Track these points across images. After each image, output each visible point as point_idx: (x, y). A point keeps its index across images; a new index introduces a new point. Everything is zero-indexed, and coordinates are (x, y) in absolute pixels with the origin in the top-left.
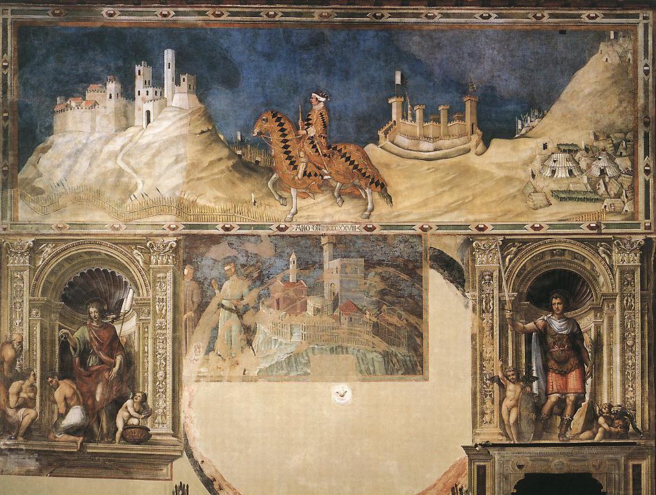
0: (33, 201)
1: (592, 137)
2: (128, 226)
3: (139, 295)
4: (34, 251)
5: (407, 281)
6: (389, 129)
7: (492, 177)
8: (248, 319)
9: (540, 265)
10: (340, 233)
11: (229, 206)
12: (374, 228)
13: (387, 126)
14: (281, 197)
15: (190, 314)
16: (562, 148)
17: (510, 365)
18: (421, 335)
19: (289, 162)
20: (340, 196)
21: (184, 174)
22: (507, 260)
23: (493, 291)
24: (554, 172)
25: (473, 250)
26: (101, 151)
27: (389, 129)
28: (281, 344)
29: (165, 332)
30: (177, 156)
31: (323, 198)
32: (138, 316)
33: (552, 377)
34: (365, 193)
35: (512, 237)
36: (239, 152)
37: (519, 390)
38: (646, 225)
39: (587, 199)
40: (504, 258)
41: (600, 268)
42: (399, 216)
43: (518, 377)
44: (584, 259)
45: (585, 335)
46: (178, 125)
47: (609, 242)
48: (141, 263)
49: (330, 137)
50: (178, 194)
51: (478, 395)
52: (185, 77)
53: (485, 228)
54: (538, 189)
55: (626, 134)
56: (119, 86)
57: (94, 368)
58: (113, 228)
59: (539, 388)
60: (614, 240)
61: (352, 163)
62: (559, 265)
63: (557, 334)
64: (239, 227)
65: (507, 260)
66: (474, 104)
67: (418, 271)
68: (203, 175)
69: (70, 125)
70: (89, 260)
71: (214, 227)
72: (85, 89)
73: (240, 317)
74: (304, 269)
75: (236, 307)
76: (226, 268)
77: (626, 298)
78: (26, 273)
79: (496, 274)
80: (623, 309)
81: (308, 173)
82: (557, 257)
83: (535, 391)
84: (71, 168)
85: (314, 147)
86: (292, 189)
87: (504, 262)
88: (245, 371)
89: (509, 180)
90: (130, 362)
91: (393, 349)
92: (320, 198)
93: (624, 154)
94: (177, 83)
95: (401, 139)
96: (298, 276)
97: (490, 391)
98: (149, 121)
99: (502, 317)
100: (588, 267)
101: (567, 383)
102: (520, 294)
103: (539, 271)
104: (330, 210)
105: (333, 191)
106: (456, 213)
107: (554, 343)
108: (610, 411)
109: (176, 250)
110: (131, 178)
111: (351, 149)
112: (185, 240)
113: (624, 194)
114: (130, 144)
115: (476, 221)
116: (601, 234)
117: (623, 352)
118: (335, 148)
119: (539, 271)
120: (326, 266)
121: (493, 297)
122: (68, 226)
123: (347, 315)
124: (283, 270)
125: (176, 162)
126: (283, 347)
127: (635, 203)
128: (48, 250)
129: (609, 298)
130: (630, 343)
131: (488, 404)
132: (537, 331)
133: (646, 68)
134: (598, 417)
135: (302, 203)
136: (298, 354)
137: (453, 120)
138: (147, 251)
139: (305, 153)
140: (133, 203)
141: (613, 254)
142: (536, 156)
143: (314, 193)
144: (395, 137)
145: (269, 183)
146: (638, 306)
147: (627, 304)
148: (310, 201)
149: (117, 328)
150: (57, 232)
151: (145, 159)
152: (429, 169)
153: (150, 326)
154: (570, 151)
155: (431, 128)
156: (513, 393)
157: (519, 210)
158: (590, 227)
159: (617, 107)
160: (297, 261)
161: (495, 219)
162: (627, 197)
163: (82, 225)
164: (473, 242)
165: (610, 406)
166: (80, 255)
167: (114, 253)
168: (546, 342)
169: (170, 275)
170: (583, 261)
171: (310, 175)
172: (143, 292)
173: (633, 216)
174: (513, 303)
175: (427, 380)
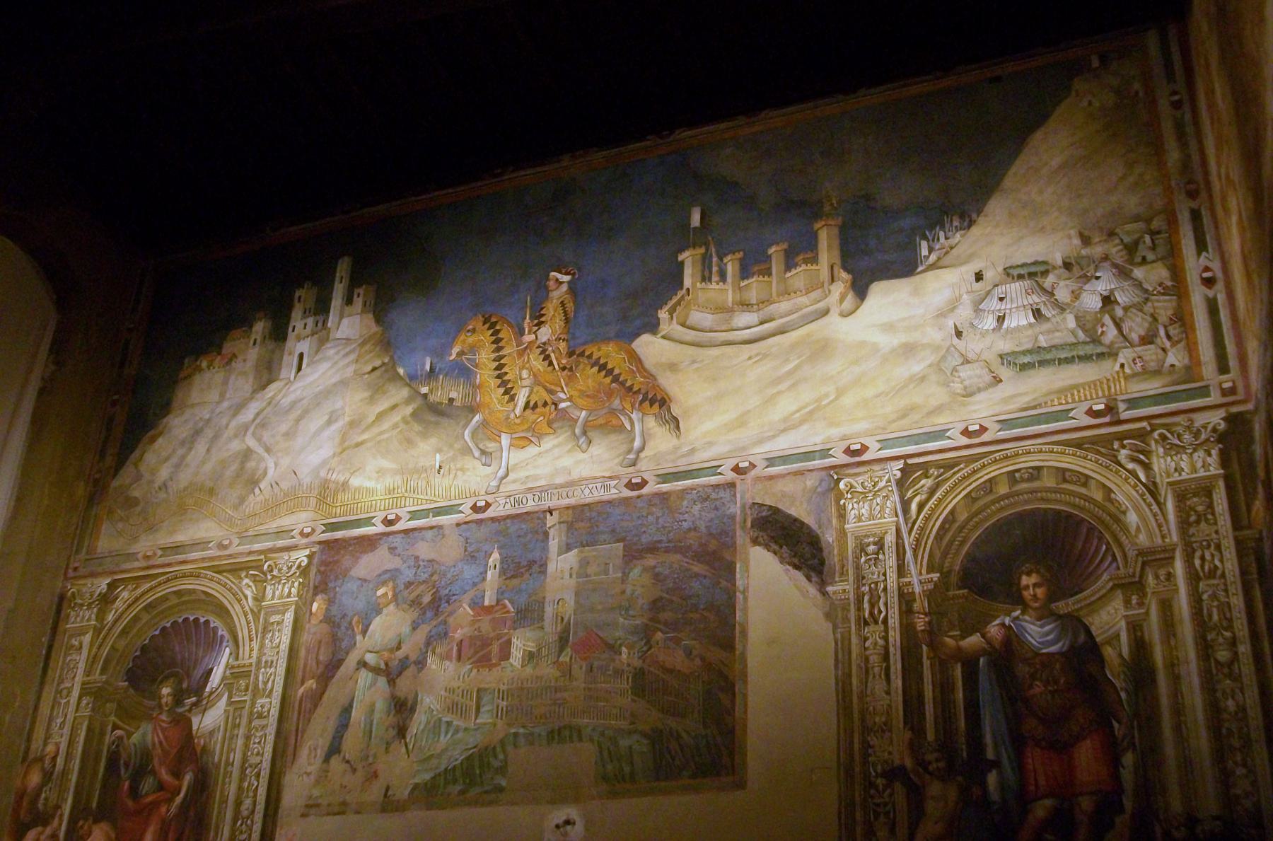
0: (121, 519)
1: (1077, 241)
2: (242, 537)
3: (237, 659)
4: (106, 600)
5: (705, 577)
6: (679, 303)
7: (875, 348)
8: (404, 685)
9: (986, 506)
10: (583, 502)
11: (398, 479)
12: (644, 483)
13: (675, 300)
14: (483, 452)
15: (311, 684)
16: (1015, 272)
17: (931, 736)
18: (729, 688)
19: (502, 390)
20: (584, 433)
21: (337, 440)
22: (914, 506)
23: (885, 575)
24: (1001, 319)
25: (840, 495)
26: (227, 425)
27: (679, 303)
28: (457, 731)
29: (264, 722)
30: (332, 413)
31: (555, 442)
32: (230, 697)
33: (1035, 759)
34: (631, 419)
35: (922, 460)
36: (424, 390)
37: (953, 794)
38: (1227, 385)
39: (1080, 358)
41: (1125, 494)
42: (693, 451)
44: (1085, 480)
45: (1108, 652)
46: (341, 364)
47: (1142, 435)
48: (250, 599)
49: (574, 338)
50: (323, 474)
51: (859, 815)
52: (361, 291)
53: (864, 449)
54: (971, 356)
55: (1148, 221)
56: (269, 324)
57: (150, 799)
58: (221, 546)
59: (1002, 787)
60: (1153, 430)
61: (610, 372)
62: (1026, 502)
63: (1038, 654)
64: (408, 516)
65: (914, 506)
66: (836, 231)
67: (727, 556)
68: (365, 437)
69: (195, 396)
70: (178, 605)
71: (368, 521)
72: (224, 339)
73: (392, 682)
74: (513, 577)
75: (387, 665)
76: (380, 592)
77: (1198, 554)
78: (87, 639)
79: (890, 539)
80: (1194, 578)
81: (532, 404)
82: (1025, 486)
84: (183, 457)
85: (547, 358)
86: (503, 436)
87: (906, 510)
88: (387, 790)
89: (909, 350)
90: (203, 786)
91: (672, 723)
92: (549, 442)
93: (1150, 257)
94: (349, 301)
95: (697, 317)
96: (501, 592)
97: (886, 805)
98: (299, 369)
99: (907, 628)
100: (1098, 496)
102: (945, 575)
104: (567, 461)
105: (573, 427)
106: (805, 427)
107: (1033, 677)
109: (304, 571)
110: (262, 459)
111: (611, 353)
112: (322, 551)
113: (1162, 332)
114: (269, 409)
115: (843, 439)
116: (1120, 422)
118: (582, 354)
119: (986, 519)
120: (551, 567)
121: (885, 589)
122: (160, 552)
123: (585, 659)
124: (475, 584)
125: (329, 422)
126: (460, 735)
127: (1192, 349)
128: (125, 594)
129: (1157, 558)
130: (1223, 655)
132: (990, 654)
133: (1176, 98)
135: (517, 456)
136: (486, 749)
137: (795, 266)
138: (259, 581)
139: (530, 370)
140: (255, 501)
141: (1154, 460)
142: (961, 296)
143: (540, 436)
144: (687, 316)
145: (467, 433)
146: (1230, 565)
147: (1202, 566)
148: (532, 450)
149: (195, 721)
150: (143, 564)
151: (284, 428)
152: (750, 358)
153: (245, 712)
154: (1031, 275)
155: (754, 287)
157: (934, 402)
158: (1091, 413)
159: (1123, 178)
160: (502, 562)
161: (884, 429)
162: (1169, 337)
163: (177, 548)
164: (839, 480)
165: (1192, 821)
166: (164, 599)
167: (215, 590)
169: (289, 617)
170: (1085, 485)
171: (536, 406)
172: (244, 650)
173: (1191, 371)
174: (930, 595)
175: (741, 785)
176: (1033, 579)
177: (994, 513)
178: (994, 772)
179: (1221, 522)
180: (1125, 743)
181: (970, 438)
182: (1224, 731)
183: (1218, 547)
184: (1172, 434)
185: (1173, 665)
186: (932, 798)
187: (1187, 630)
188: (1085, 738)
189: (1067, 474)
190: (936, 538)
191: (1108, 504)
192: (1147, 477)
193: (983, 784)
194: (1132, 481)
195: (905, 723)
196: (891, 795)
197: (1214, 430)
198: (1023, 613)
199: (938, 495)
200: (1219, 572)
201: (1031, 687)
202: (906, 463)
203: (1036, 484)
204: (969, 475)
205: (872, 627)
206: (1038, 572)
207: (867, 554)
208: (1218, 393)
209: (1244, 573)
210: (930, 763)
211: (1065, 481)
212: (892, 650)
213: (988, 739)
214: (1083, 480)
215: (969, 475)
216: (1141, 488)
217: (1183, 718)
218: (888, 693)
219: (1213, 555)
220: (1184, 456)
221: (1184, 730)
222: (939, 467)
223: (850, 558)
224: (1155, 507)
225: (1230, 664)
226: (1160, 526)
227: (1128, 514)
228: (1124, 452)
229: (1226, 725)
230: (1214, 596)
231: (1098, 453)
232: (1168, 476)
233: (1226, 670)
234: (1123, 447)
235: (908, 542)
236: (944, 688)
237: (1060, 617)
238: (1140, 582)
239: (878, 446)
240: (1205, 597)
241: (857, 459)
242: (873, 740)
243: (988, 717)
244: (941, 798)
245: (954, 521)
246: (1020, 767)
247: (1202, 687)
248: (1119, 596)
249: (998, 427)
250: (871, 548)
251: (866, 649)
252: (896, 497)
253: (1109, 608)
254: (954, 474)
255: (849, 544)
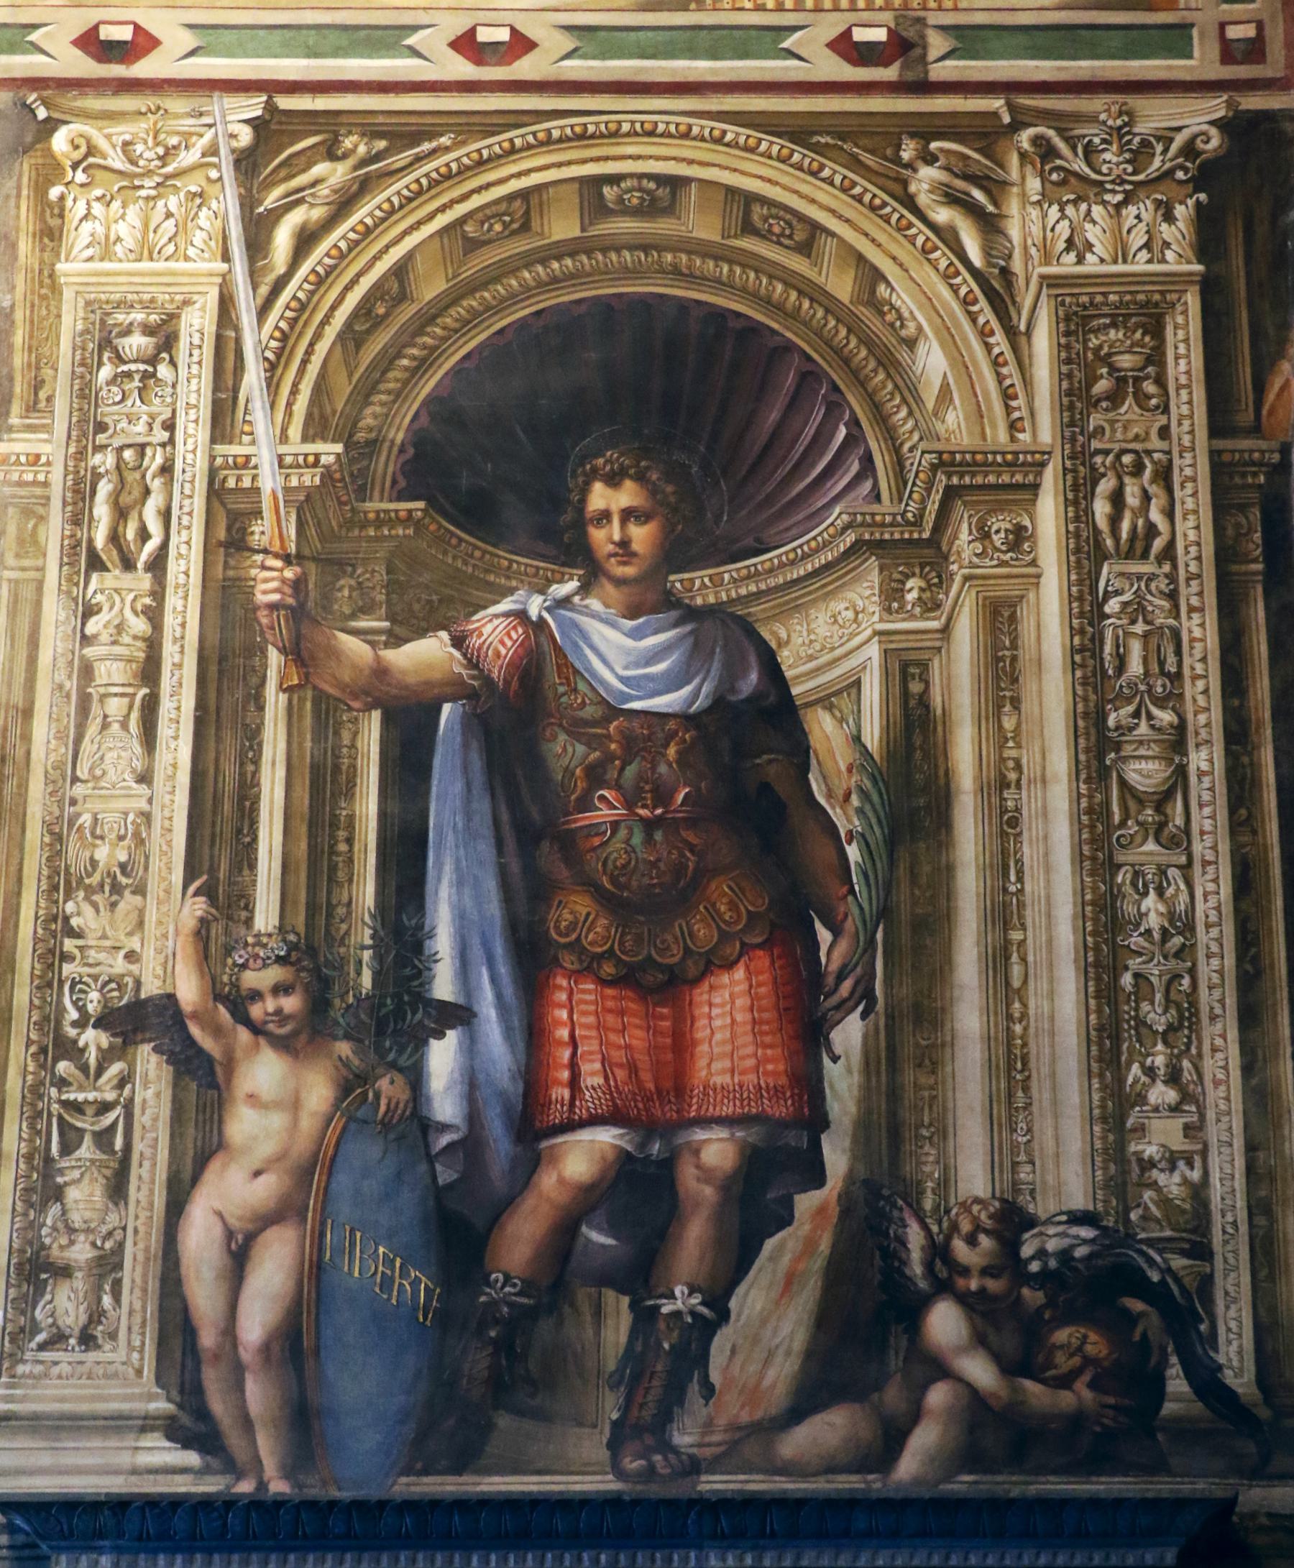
17: (265, 916)
22: (283, 238)
23: (170, 426)
25: (51, 171)
33: (576, 1009)
37: (318, 1092)
38: (1234, 32)
40: (257, 233)
41: (920, 292)
43: (318, 1005)
44: (809, 237)
45: (824, 729)
47: (987, 135)
53: (143, 43)
59: (472, 1083)
60: (1016, 126)
63: (614, 712)
65: (283, 238)
77: (1106, 486)
79: (198, 323)
80: (1086, 552)
83: (445, 1104)
87: (257, 245)
97: (105, 1107)
99: (225, 596)
100: (842, 286)
101: (681, 1044)
102: (361, 451)
103: (513, 299)
108: (1008, 1260)
116: (925, 87)
117: (1098, 852)
121: (166, 470)
129: (985, 483)
130: (1145, 772)
131: (84, 1194)
132: (471, 695)
134: (911, 1312)
141: (1013, 207)
146: (1193, 528)
147: (1115, 521)
156: (277, 1120)
158: (844, 46)
164: (51, 125)
165: (1012, 1220)
168: (535, 761)
170: (805, 249)
174: (306, 505)
176: (627, 496)
177: (527, 292)
178: (452, 1036)
179: (1178, 407)
180: (846, 986)
181: (479, 62)
182: (1127, 980)
183: (1164, 475)
184: (1071, 142)
185: (1003, 784)
186: (252, 1098)
187: (1051, 693)
188: (730, 966)
189: (758, 211)
190: (341, 337)
191: (865, 312)
192: (987, 252)
193: (416, 1078)
194: (943, 257)
195: (191, 872)
196: (122, 1082)
197: (1189, 150)
198: (585, 589)
199: (363, 213)
200: (1158, 544)
201: (585, 804)
202: (270, 107)
203: (662, 227)
204: (464, 171)
205: (114, 578)
206: (640, 478)
207: (120, 359)
208: (1214, 51)
209: (1226, 555)
210: (256, 995)
211: (748, 228)
212: (169, 651)
213: (443, 943)
214: (800, 236)
215: (464, 171)
216: (968, 284)
217: (1016, 936)
218: (145, 778)
219: (1146, 497)
220: (1097, 211)
221: (1016, 970)
222: (373, 133)
223: (64, 365)
224: (999, 340)
225: (1162, 800)
226: (1007, 396)
227: (921, 349)
228: (928, 174)
229: (1134, 963)
230: (1137, 610)
231: (855, 164)
232: (1047, 258)
233: (1149, 814)
234: (930, 159)
235: (254, 339)
236: (324, 785)
237: (692, 614)
238: (934, 542)
239: (189, 40)
240: (1113, 606)
241: (117, 70)
242: (82, 914)
243: (448, 868)
244: (277, 1101)
245: (403, 297)
246: (533, 1036)
247: (1079, 858)
248: (871, 576)
249: (568, 43)
250: (136, 343)
251: (86, 640)
252: (228, 201)
253: (838, 605)
254: (418, 159)
255: (67, 320)
